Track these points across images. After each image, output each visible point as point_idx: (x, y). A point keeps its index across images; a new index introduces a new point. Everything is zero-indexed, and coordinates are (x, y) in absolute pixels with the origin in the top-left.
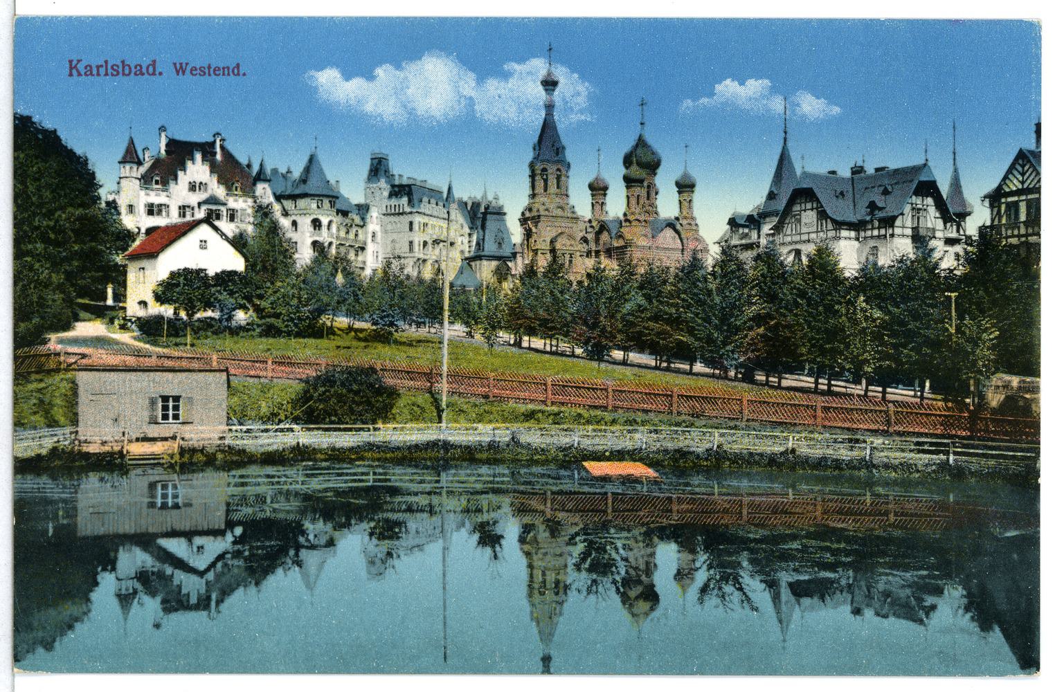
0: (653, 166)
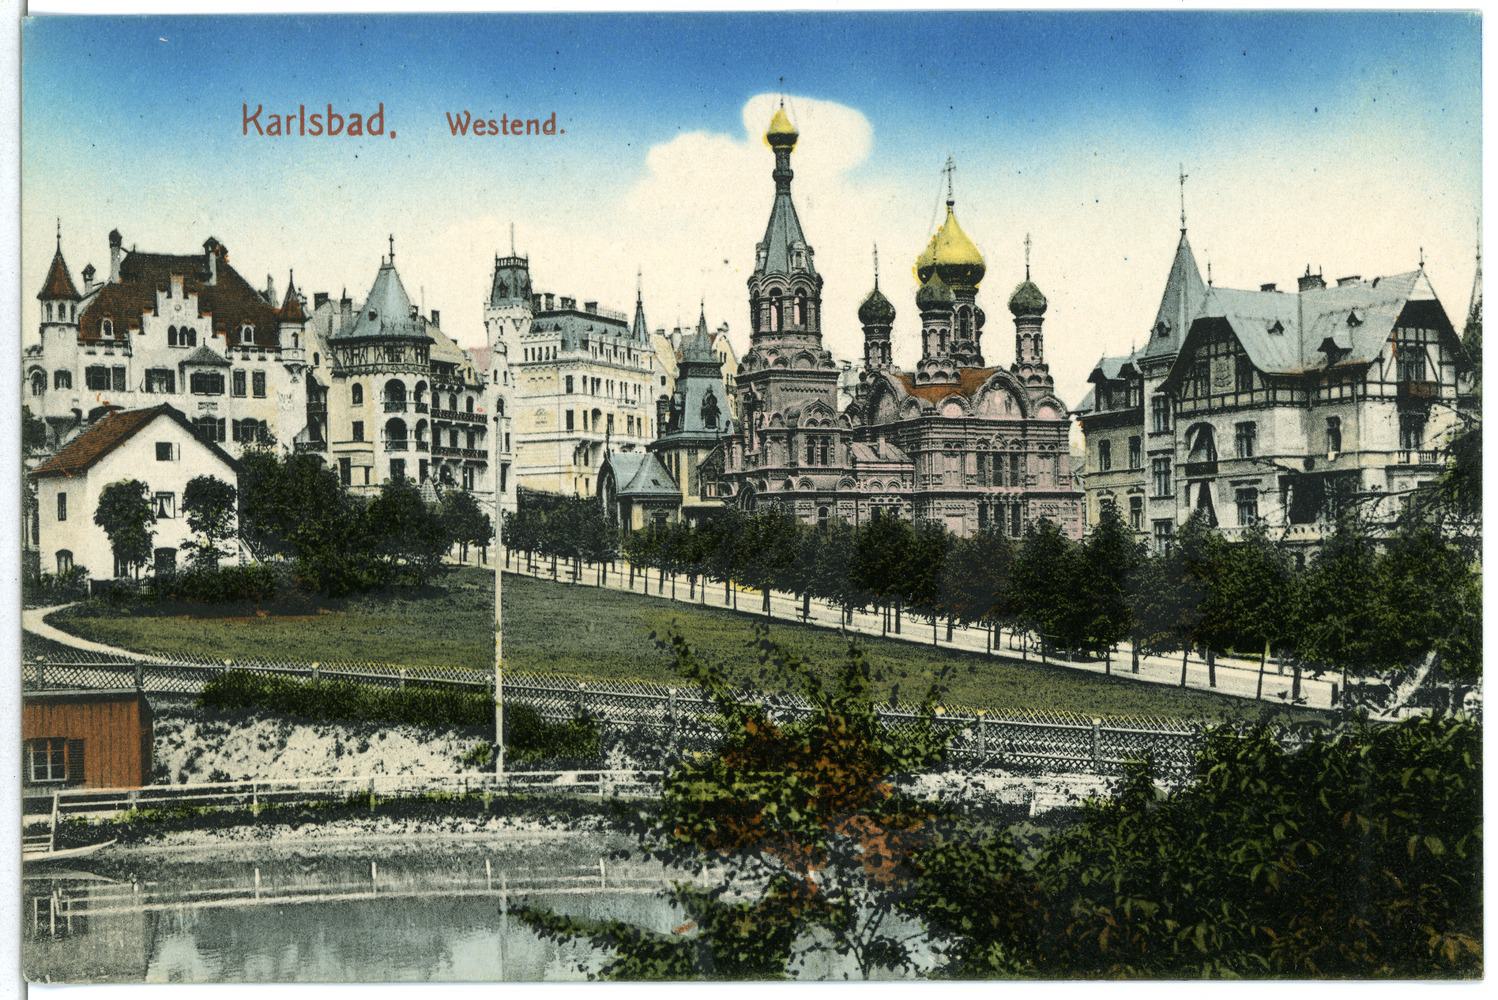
0: (968, 275)
